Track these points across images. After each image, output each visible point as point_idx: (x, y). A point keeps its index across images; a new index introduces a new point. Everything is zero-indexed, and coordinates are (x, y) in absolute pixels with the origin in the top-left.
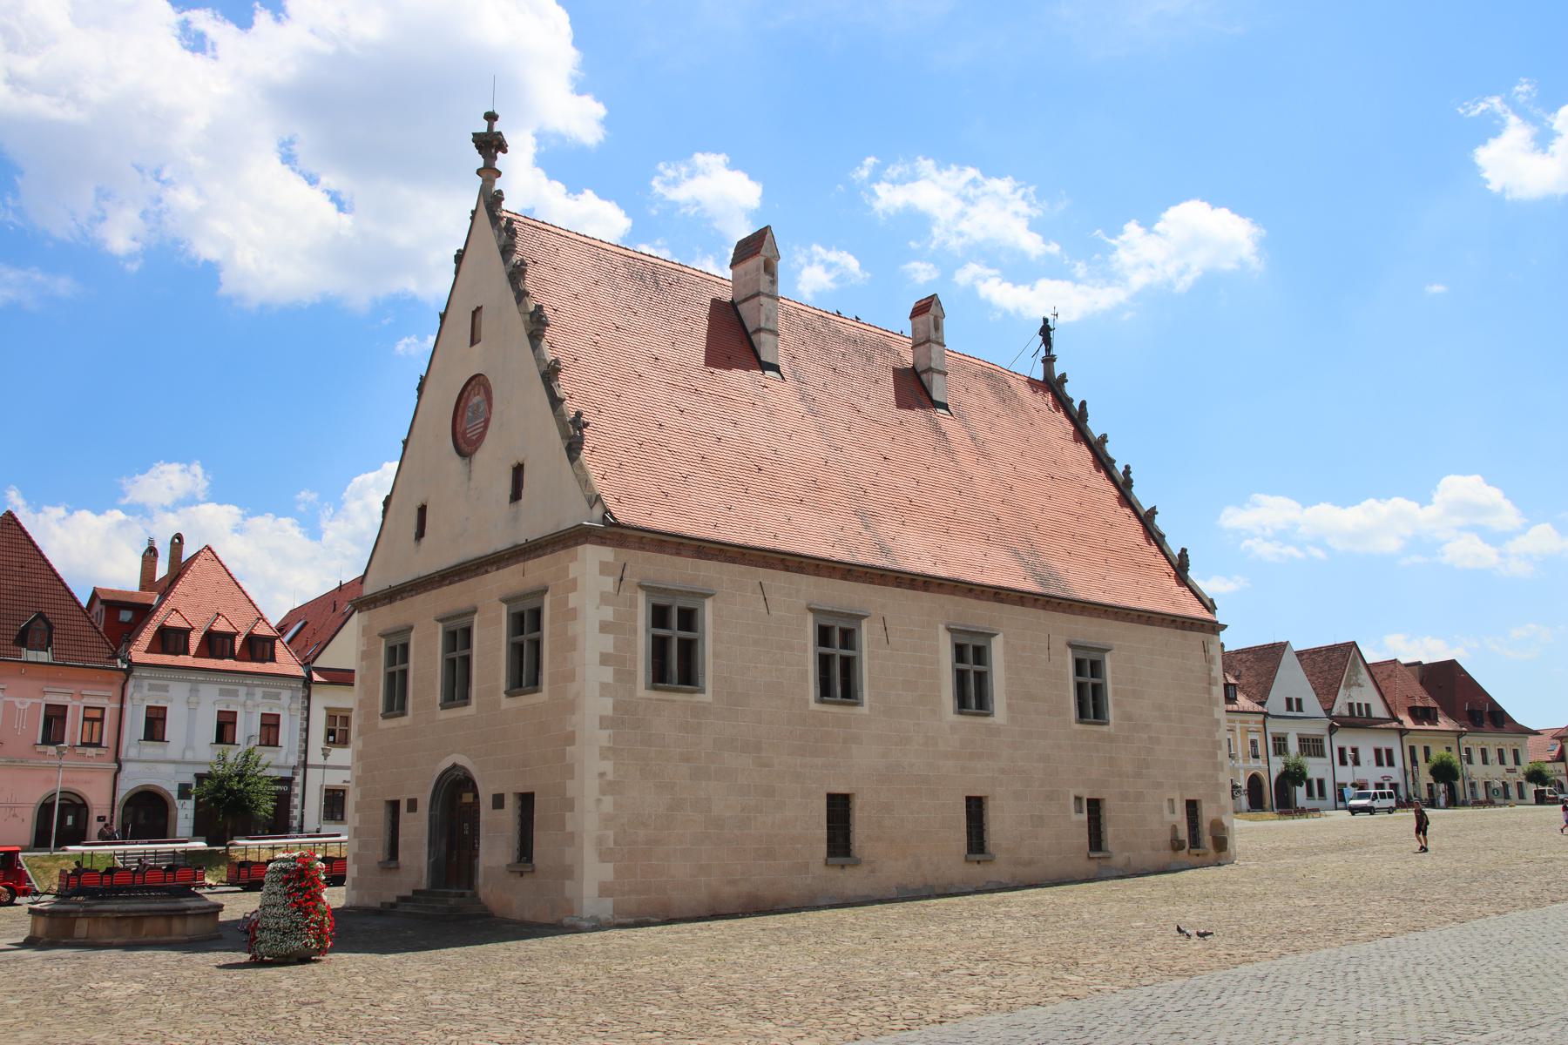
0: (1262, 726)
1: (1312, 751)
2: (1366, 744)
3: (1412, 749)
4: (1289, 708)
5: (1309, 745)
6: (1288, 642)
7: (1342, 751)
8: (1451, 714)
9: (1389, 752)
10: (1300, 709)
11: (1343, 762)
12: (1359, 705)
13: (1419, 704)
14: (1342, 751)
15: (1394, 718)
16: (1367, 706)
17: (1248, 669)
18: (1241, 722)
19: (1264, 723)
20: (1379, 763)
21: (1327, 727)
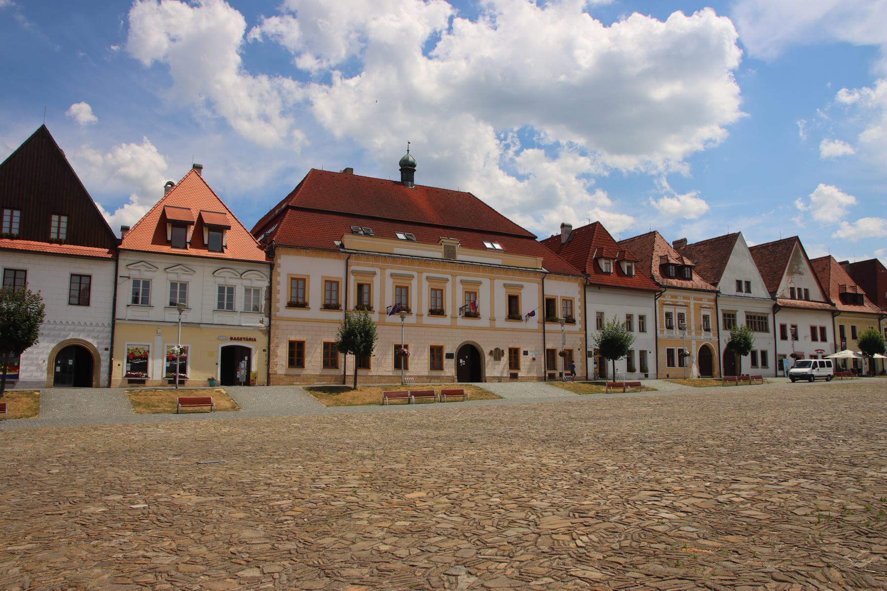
0: (713, 303)
1: (757, 326)
2: (804, 324)
3: (842, 328)
4: (739, 289)
5: (755, 322)
6: (740, 232)
7: (783, 327)
8: (874, 300)
9: (823, 330)
10: (748, 290)
11: (784, 337)
12: (799, 289)
13: (849, 291)
14: (783, 327)
15: (828, 301)
16: (806, 290)
17: (705, 257)
18: (695, 299)
19: (716, 301)
20: (814, 339)
21: (771, 306)
